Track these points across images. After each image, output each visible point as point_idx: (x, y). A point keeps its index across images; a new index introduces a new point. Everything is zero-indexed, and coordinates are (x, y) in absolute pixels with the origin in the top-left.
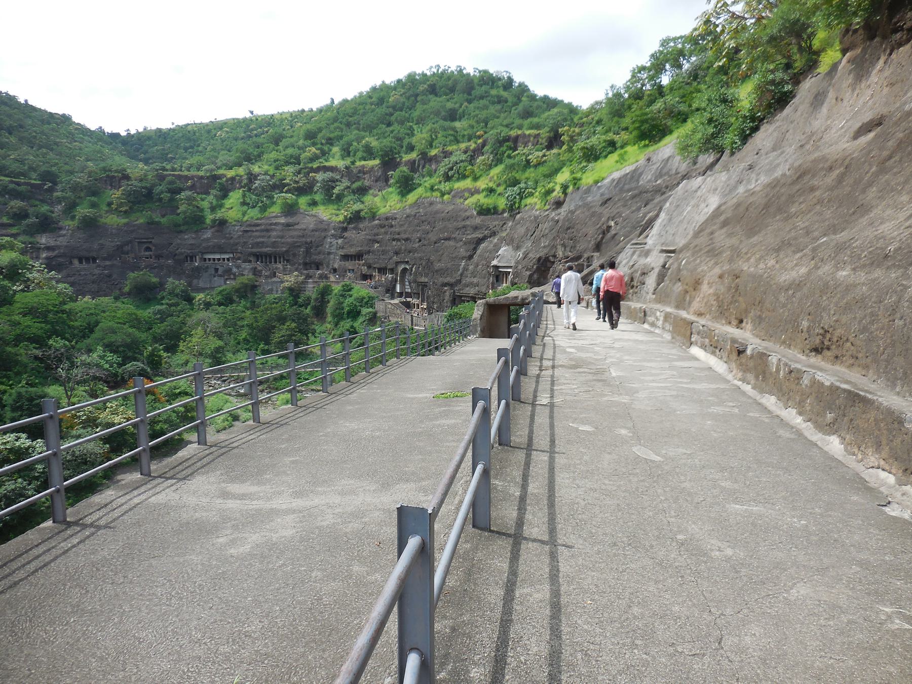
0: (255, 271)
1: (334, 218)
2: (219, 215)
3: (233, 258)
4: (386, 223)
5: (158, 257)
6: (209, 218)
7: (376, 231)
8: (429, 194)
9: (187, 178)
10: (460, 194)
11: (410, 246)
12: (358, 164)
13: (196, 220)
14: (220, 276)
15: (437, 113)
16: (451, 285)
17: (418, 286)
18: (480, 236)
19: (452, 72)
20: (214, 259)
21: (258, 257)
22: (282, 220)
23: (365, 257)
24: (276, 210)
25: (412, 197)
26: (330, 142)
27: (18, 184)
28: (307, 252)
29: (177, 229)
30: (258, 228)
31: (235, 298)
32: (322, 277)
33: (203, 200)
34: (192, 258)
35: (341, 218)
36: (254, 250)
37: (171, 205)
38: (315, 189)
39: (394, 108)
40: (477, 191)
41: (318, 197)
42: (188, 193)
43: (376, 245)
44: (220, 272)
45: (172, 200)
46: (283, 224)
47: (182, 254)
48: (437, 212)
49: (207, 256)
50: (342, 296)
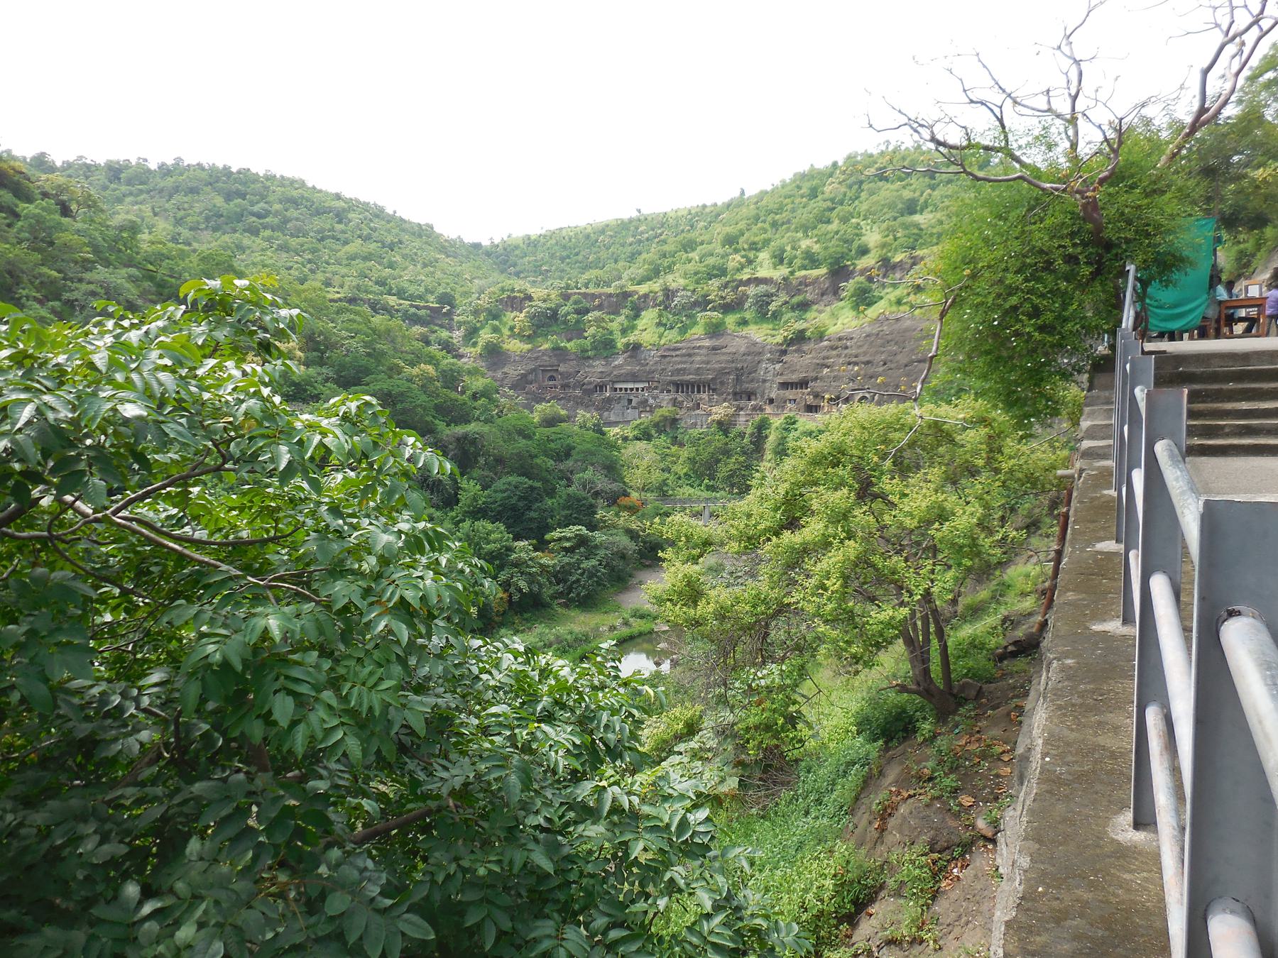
0: (675, 402)
1: (770, 339)
2: (632, 338)
4: (840, 343)
5: (564, 387)
6: (620, 342)
7: (825, 353)
8: (894, 308)
9: (594, 296)
11: (871, 370)
12: (798, 274)
13: (605, 346)
14: (634, 408)
15: (891, 206)
19: (907, 149)
21: (679, 386)
22: (707, 343)
24: (698, 330)
25: (872, 312)
26: (754, 247)
27: (418, 308)
29: (583, 357)
31: (653, 432)
32: (754, 408)
33: (612, 321)
34: (601, 387)
35: (779, 339)
36: (675, 378)
37: (577, 331)
38: (747, 305)
39: (832, 200)
41: (748, 315)
42: (597, 313)
43: (826, 370)
44: (634, 404)
45: (578, 322)
47: (590, 383)
48: (906, 330)
49: (618, 386)
50: (785, 429)
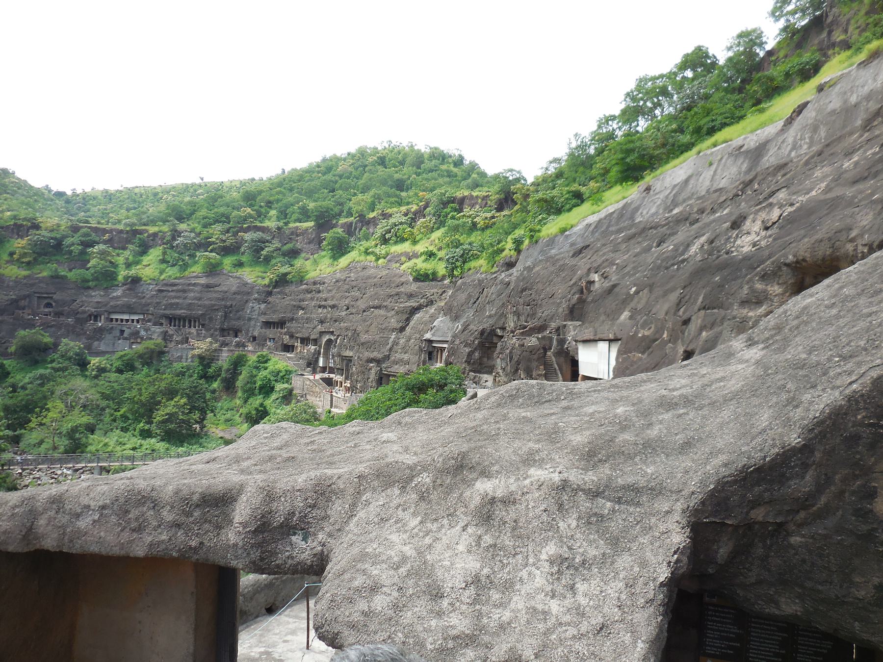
0: (166, 337)
1: (260, 281)
2: (133, 272)
3: (143, 320)
4: (314, 288)
5: (58, 314)
6: (122, 274)
7: (301, 296)
8: (362, 258)
9: (104, 231)
10: (396, 259)
11: (336, 314)
12: (291, 225)
13: (107, 277)
14: (126, 339)
15: (384, 183)
16: (378, 362)
17: (343, 360)
18: (415, 304)
20: (122, 320)
21: (171, 319)
22: (203, 281)
23: (288, 325)
24: (197, 269)
25: (344, 261)
28: (226, 316)
29: (84, 286)
30: (174, 288)
31: (137, 364)
32: (238, 345)
33: (118, 255)
34: (96, 317)
35: (267, 281)
36: (168, 312)
37: (82, 260)
38: (242, 250)
39: (341, 177)
40: (416, 256)
41: (244, 259)
42: (102, 247)
43: (301, 312)
44: (125, 335)
45: (83, 253)
46: (202, 285)
47: (84, 312)
48: (369, 277)
49: (114, 316)
50: (257, 368)
